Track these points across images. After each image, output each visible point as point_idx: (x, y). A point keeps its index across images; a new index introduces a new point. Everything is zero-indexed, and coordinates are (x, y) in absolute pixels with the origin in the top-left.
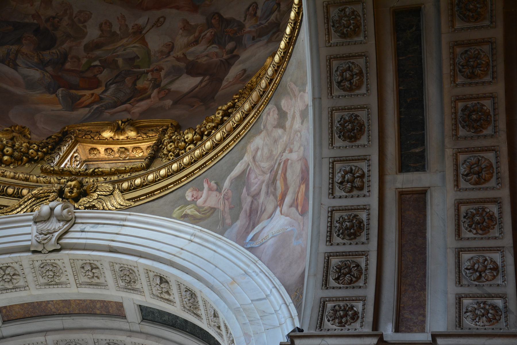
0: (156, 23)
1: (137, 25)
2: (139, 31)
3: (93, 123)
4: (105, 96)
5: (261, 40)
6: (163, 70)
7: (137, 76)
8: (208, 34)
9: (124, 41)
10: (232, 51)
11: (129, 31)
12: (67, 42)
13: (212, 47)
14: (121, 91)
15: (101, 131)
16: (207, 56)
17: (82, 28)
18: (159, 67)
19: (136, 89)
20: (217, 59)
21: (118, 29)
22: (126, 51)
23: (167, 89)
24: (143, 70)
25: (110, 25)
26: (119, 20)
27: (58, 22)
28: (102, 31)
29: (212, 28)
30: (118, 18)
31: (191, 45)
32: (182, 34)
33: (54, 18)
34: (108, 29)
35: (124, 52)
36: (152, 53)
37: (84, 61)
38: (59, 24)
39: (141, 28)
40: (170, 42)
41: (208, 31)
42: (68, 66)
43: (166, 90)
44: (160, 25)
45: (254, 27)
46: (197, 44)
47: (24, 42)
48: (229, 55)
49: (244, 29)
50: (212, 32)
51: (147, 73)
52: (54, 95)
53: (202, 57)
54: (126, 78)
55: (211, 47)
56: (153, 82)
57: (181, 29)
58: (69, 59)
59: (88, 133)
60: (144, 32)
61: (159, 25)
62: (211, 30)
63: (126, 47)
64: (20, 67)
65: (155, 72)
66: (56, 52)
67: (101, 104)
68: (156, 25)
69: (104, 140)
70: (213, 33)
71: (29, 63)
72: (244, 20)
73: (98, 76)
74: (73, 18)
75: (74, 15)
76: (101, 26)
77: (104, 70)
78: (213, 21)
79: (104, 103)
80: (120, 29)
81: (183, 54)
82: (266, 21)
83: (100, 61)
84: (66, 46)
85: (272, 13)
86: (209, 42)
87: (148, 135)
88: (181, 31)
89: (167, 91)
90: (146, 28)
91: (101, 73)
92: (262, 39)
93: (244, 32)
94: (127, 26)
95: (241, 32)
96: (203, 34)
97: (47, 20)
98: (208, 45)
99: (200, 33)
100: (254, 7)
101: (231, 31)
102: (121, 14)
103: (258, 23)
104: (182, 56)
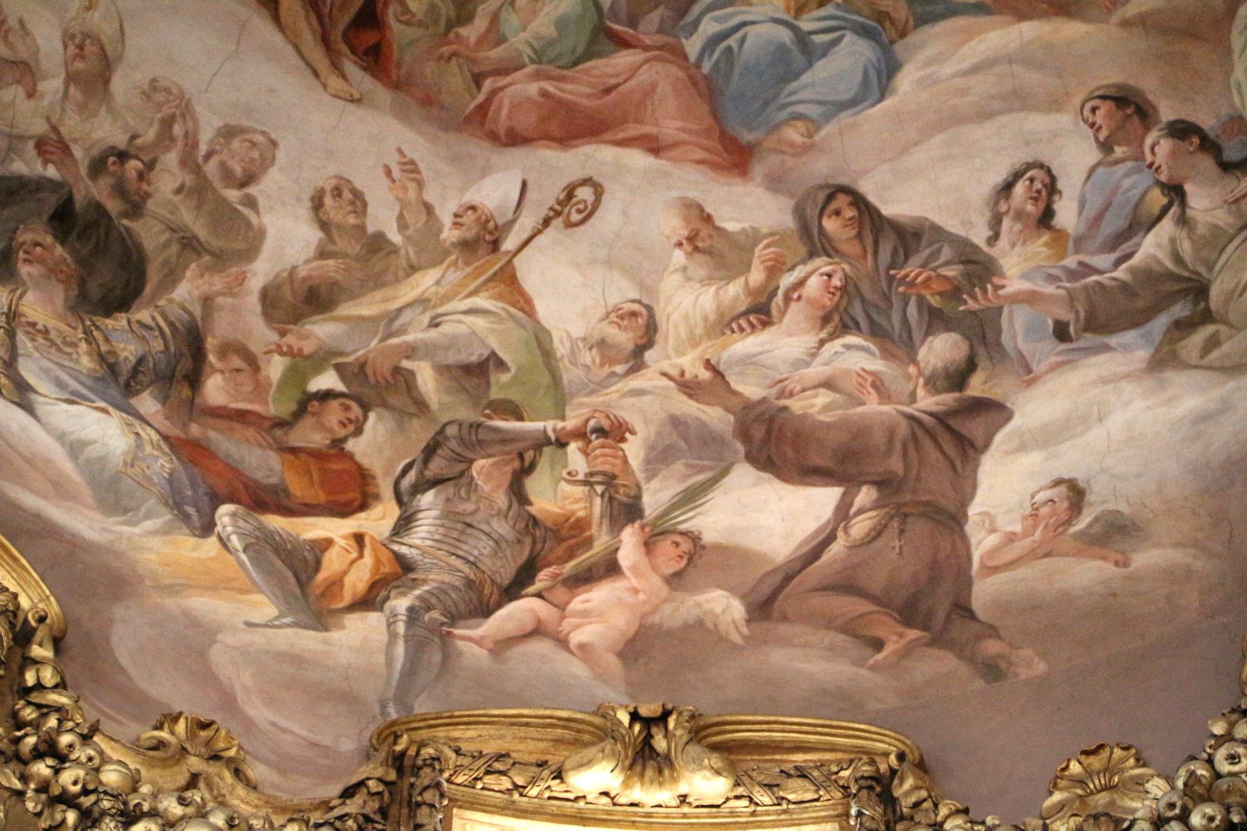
0: (558, 208)
1: (473, 208)
2: (488, 237)
3: (497, 712)
4: (413, 551)
5: (1107, 348)
6: (633, 433)
7: (521, 456)
8: (814, 283)
9: (426, 281)
10: (958, 378)
11: (443, 236)
12: (189, 274)
13: (848, 347)
14: (470, 525)
15: (567, 765)
16: (828, 384)
17: (240, 208)
18: (608, 417)
19: (535, 521)
20: (886, 408)
21: (395, 225)
22: (440, 329)
23: (683, 534)
24: (538, 425)
25: (359, 202)
26: (394, 181)
27: (141, 176)
28: (324, 226)
29: (829, 256)
30: (388, 172)
31: (734, 325)
32: (684, 269)
33: (123, 156)
34: (352, 220)
35: (433, 334)
36: (561, 349)
37: (276, 368)
38: (145, 187)
39: (496, 227)
40: (633, 301)
41: (810, 267)
42: (215, 390)
43: (678, 539)
44: (580, 217)
45: (1052, 279)
46: (766, 324)
47: (24, 270)
48: (948, 399)
49: (996, 280)
50: (829, 276)
51: (561, 444)
52: (213, 540)
53: (804, 390)
54: (471, 461)
55: (836, 345)
56: (599, 489)
57: (680, 245)
58: (212, 358)
59: (498, 766)
60: (509, 244)
61: (575, 217)
62: (821, 264)
63: (440, 310)
64: (41, 399)
65: (596, 441)
66: (153, 318)
67: (417, 592)
68: (560, 219)
69: (568, 800)
70: (836, 282)
71: (65, 377)
72: (994, 239)
73: (350, 445)
74: (200, 160)
75: (203, 148)
76: (317, 204)
77: (366, 418)
78: (830, 224)
79: (426, 588)
80: (402, 224)
81: (708, 364)
82: (1113, 257)
83: (339, 368)
84: (186, 291)
85: (1139, 224)
86: (826, 320)
87: (782, 794)
88: (679, 256)
89: (686, 546)
90: (517, 226)
91: (358, 431)
92: (1113, 340)
93: (1001, 292)
94: (429, 209)
95: (985, 291)
96: (787, 280)
97: (97, 167)
98: (823, 335)
99: (775, 269)
100: (1037, 185)
101: (929, 279)
102: (400, 152)
103: (1071, 262)
104: (705, 375)
